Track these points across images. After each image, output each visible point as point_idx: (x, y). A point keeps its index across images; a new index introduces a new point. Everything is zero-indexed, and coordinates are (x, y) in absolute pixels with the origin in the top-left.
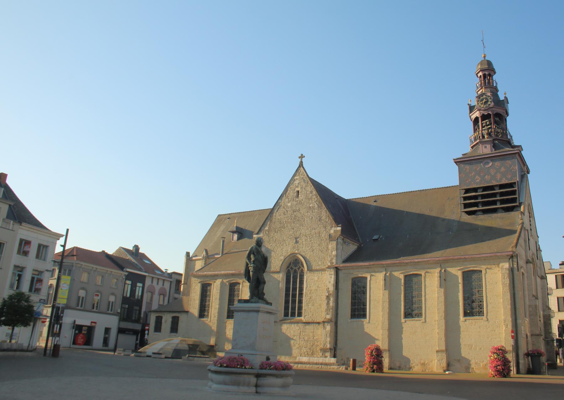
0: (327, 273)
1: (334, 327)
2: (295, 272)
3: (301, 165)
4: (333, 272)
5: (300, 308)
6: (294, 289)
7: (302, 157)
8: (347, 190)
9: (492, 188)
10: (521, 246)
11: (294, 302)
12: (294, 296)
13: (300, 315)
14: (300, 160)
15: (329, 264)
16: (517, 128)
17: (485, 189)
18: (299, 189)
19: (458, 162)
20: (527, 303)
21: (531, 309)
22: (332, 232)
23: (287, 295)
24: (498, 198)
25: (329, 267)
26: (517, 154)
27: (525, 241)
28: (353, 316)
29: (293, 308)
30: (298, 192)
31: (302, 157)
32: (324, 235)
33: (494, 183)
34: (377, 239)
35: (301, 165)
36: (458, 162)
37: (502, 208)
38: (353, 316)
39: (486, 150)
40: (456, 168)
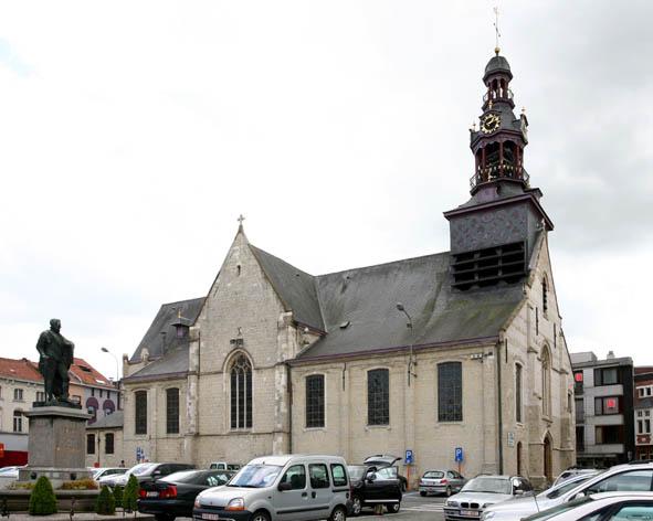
0: (277, 372)
1: (286, 438)
2: (241, 372)
3: (241, 231)
4: (283, 368)
5: (250, 416)
6: (241, 393)
7: (241, 219)
8: (316, 260)
9: (492, 251)
10: (518, 329)
11: (241, 409)
12: (241, 402)
13: (250, 425)
14: (239, 224)
15: (279, 360)
16: (536, 164)
17: (484, 252)
18: (239, 263)
19: (450, 216)
20: (525, 401)
21: (530, 411)
22: (281, 318)
23: (233, 401)
24: (500, 264)
25: (279, 364)
26: (531, 199)
27: (528, 323)
28: (309, 424)
29: (241, 417)
30: (239, 267)
31: (241, 219)
32: (272, 325)
33: (496, 243)
34: (345, 327)
35: (241, 231)
36: (450, 216)
37: (504, 279)
38: (309, 424)
39: (489, 196)
40: (447, 222)
